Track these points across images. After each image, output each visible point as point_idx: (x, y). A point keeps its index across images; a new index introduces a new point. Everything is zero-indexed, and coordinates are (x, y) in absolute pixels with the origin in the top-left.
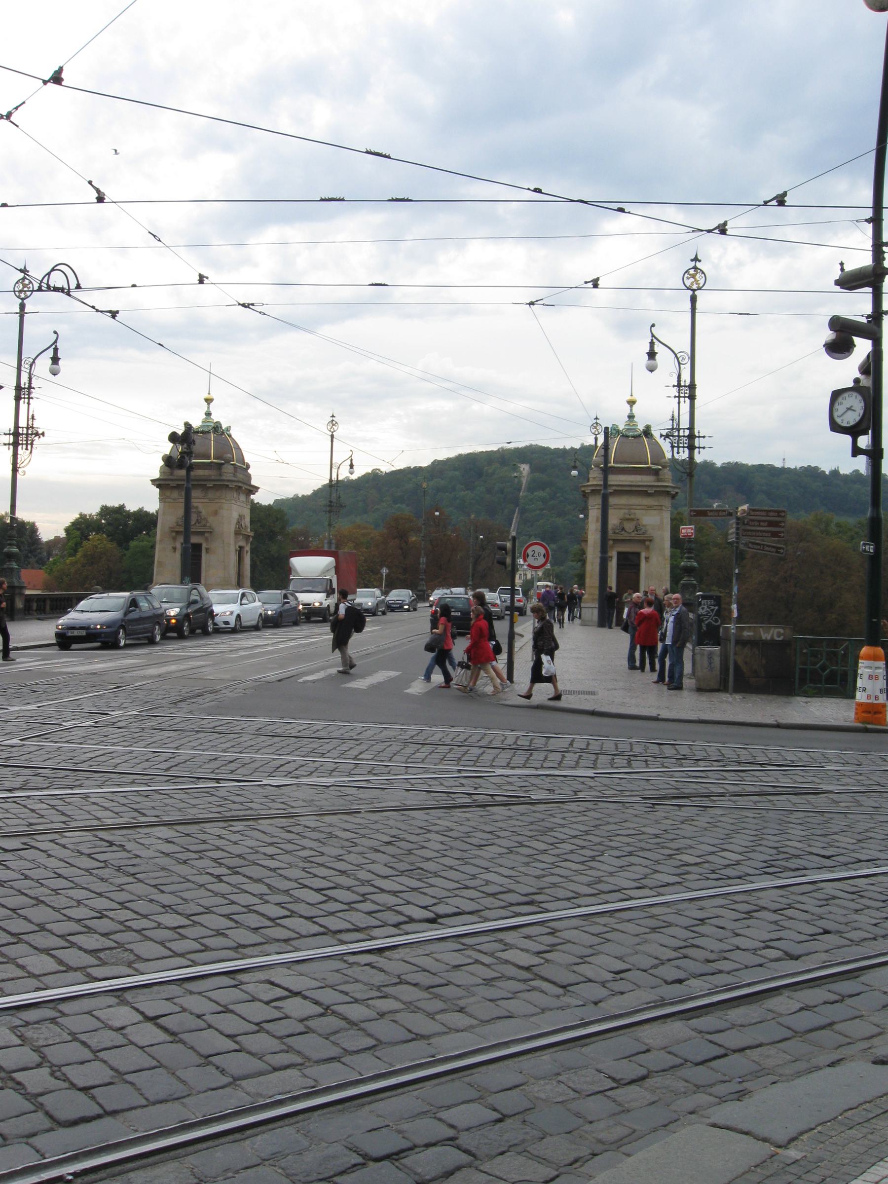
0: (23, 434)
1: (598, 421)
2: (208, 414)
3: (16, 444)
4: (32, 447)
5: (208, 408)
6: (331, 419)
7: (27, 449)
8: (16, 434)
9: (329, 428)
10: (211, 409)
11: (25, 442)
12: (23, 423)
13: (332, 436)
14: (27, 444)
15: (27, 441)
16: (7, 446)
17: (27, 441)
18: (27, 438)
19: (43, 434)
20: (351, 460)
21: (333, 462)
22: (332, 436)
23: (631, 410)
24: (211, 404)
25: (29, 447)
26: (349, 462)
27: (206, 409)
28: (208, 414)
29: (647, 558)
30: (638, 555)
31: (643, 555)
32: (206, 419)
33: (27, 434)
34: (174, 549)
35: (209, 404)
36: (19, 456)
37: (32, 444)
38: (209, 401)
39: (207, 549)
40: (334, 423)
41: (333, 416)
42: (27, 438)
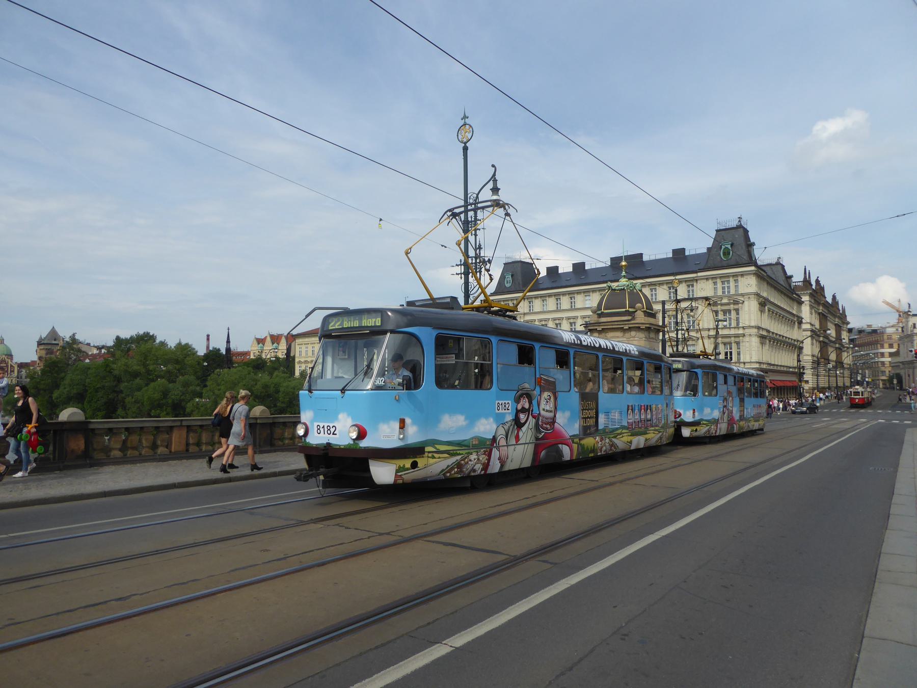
13: (465, 149)
20: (495, 181)
22: (465, 149)
26: (491, 185)
41: (465, 117)
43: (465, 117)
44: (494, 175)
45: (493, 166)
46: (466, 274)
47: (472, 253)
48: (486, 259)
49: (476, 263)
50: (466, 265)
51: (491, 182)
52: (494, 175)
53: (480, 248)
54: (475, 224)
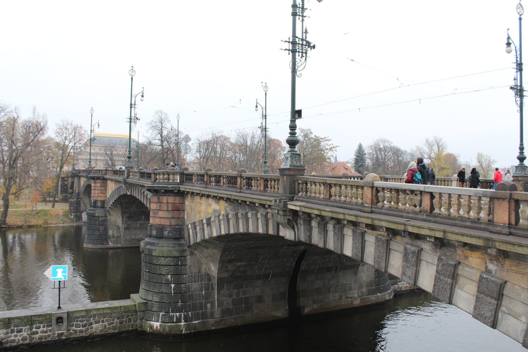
0: (299, 44)
3: (294, 51)
4: (306, 56)
7: (302, 56)
8: (294, 43)
11: (301, 51)
12: (299, 34)
14: (302, 53)
15: (302, 49)
16: (288, 52)
17: (302, 49)
18: (302, 47)
19: (314, 47)
25: (304, 55)
33: (302, 45)
36: (297, 63)
37: (306, 53)
42: (302, 47)
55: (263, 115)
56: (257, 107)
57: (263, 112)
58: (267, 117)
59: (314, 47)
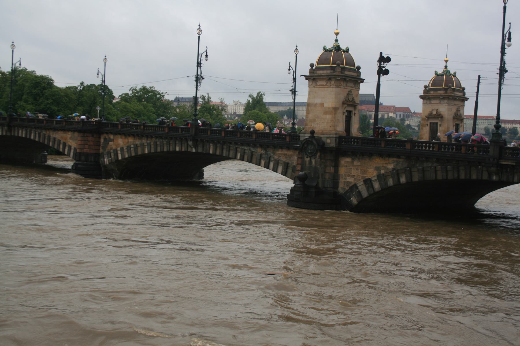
1: (297, 48)
2: (336, 41)
5: (337, 38)
6: (199, 27)
9: (198, 32)
10: (338, 38)
13: (199, 37)
20: (207, 53)
21: (199, 52)
22: (199, 37)
23: (446, 64)
24: (338, 35)
26: (205, 54)
27: (335, 38)
28: (336, 41)
29: (461, 126)
30: (437, 123)
31: (460, 125)
32: (335, 43)
34: (344, 113)
35: (337, 35)
38: (337, 34)
39: (355, 114)
40: (200, 29)
43: (199, 26)
44: (207, 50)
45: (207, 47)
46: (197, 81)
47: (199, 73)
48: (203, 77)
49: (200, 78)
50: (197, 78)
51: (205, 53)
52: (207, 50)
53: (201, 73)
54: (201, 65)
55: (293, 78)
56: (289, 70)
57: (293, 76)
58: (297, 80)
59: (507, 71)
